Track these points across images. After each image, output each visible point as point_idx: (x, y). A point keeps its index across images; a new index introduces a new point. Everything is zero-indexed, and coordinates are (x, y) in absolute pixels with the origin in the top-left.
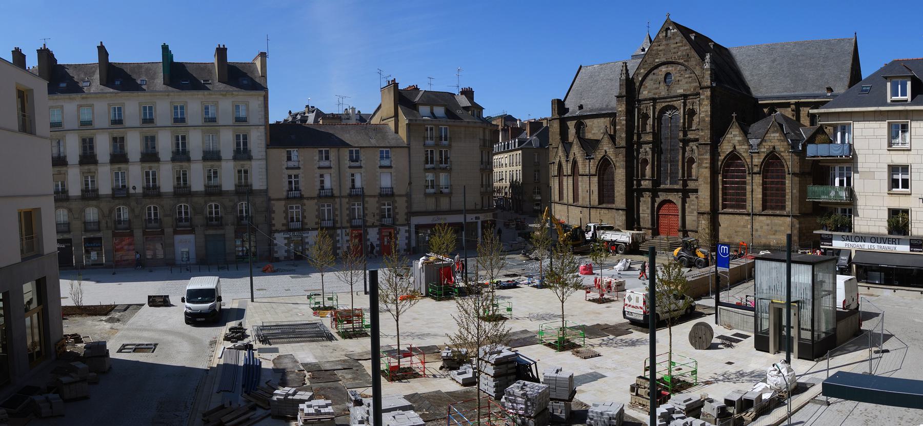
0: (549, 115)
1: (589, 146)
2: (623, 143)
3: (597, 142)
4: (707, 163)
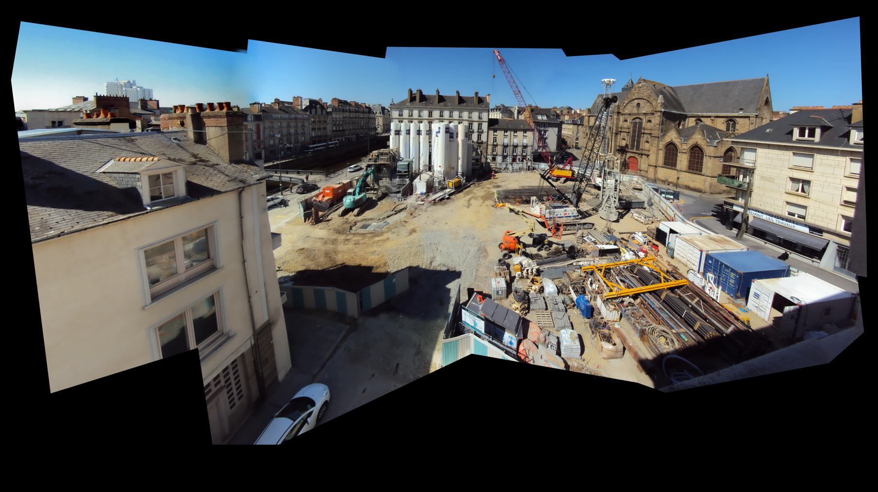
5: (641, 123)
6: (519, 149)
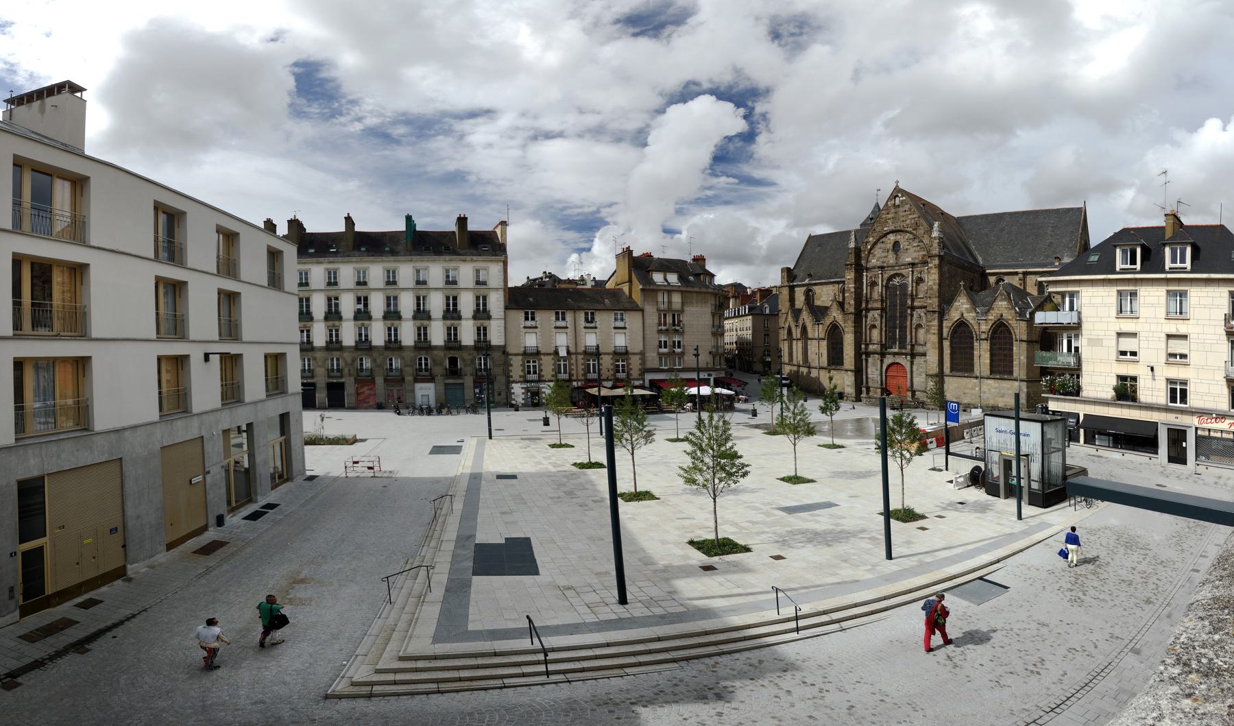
0: (779, 283)
1: (819, 313)
2: (852, 310)
3: (827, 308)
4: (935, 330)
5: (904, 287)
6: (607, 361)
